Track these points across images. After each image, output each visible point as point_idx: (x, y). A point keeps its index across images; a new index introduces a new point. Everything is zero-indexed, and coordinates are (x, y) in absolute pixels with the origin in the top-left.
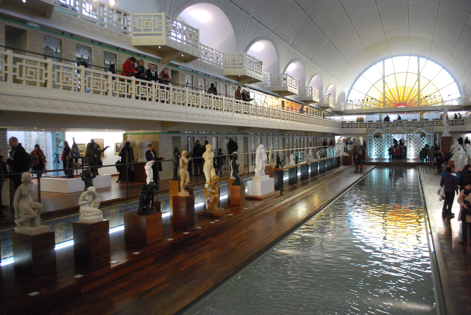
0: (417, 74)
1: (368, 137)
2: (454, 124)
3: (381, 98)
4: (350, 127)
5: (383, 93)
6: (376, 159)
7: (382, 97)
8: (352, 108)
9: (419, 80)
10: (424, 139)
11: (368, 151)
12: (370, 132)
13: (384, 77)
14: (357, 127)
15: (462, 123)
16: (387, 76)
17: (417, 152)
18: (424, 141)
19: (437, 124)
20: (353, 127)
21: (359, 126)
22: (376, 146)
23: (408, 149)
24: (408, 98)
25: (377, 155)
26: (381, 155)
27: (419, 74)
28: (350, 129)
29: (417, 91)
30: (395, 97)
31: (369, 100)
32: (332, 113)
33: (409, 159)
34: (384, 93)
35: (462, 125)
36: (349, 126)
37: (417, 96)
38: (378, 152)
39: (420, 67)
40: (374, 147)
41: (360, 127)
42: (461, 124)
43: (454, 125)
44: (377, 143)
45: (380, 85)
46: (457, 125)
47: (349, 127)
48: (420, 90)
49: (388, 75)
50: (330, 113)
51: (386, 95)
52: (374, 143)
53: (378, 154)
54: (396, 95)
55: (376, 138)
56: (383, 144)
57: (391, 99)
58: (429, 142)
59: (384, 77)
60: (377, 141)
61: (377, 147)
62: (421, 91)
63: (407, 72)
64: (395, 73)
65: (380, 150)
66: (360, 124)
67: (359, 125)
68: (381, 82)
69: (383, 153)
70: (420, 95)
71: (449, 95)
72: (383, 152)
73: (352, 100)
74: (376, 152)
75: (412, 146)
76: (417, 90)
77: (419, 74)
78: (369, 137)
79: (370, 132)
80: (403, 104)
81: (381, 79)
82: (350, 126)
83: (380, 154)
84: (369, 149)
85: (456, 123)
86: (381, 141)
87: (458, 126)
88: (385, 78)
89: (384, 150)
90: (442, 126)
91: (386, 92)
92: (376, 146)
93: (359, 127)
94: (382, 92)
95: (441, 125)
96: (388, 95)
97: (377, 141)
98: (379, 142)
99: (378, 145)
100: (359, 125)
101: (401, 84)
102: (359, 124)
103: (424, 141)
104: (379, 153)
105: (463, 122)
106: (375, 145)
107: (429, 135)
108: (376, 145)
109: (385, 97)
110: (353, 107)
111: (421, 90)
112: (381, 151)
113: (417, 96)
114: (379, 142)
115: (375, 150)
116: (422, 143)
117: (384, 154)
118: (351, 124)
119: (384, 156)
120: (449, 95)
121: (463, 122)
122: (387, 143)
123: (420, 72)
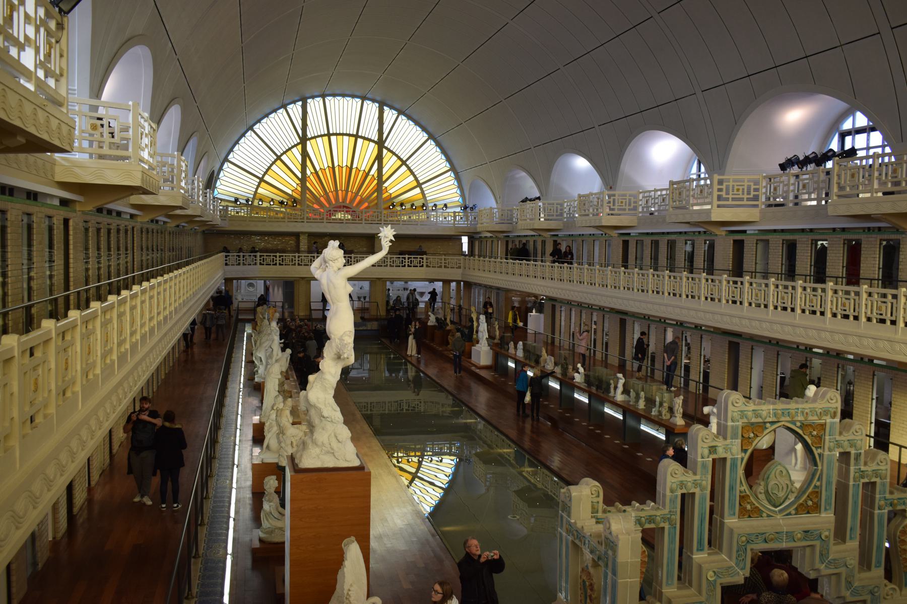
7: (299, 189)
9: (379, 158)
13: (304, 140)
16: (312, 138)
27: (380, 143)
29: (376, 182)
30: (328, 191)
37: (376, 194)
45: (294, 158)
49: (315, 137)
51: (308, 185)
54: (329, 186)
59: (304, 140)
63: (357, 136)
64: (329, 135)
68: (297, 152)
70: (382, 190)
77: (380, 143)
81: (298, 144)
88: (308, 142)
94: (300, 176)
111: (384, 178)
113: (376, 194)
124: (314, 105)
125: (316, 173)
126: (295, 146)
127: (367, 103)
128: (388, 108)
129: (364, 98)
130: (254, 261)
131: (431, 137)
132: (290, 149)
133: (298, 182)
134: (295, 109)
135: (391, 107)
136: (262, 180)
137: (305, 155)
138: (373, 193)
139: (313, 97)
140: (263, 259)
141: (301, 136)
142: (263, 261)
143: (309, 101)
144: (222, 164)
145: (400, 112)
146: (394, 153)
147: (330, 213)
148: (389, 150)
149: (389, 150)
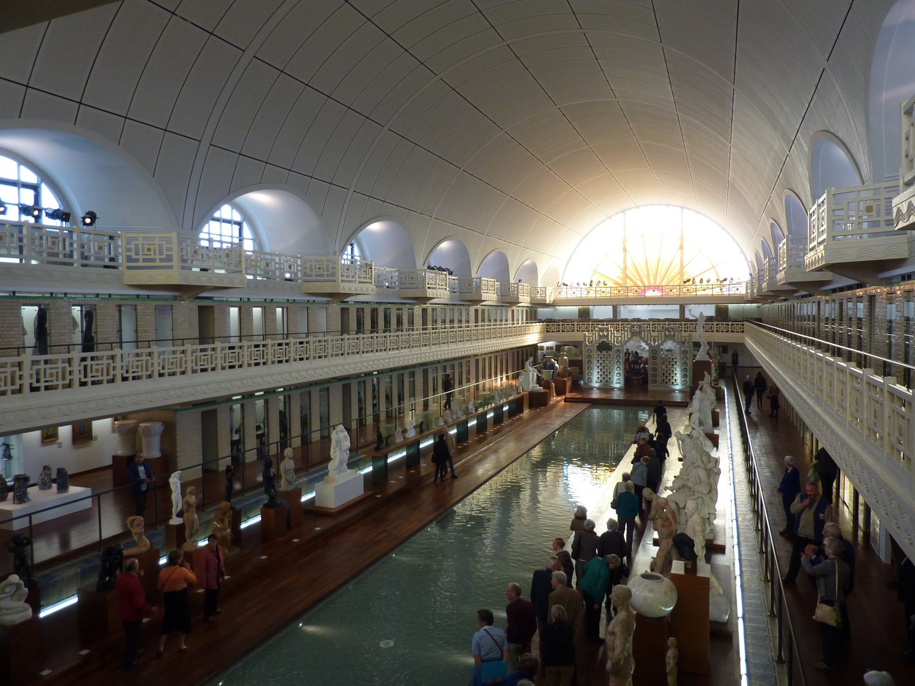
2: (730, 329)
3: (619, 277)
5: (622, 268)
7: (622, 276)
9: (681, 247)
14: (573, 331)
21: (576, 329)
24: (664, 278)
26: (607, 381)
29: (679, 266)
31: (594, 285)
34: (625, 268)
37: (679, 276)
38: (603, 376)
40: (596, 368)
41: (578, 331)
44: (600, 362)
47: (559, 331)
48: (684, 265)
51: (628, 272)
52: (596, 362)
55: (599, 353)
56: (610, 363)
57: (643, 273)
58: (686, 363)
61: (600, 368)
65: (606, 374)
66: (578, 325)
69: (610, 378)
70: (683, 273)
71: (725, 280)
73: (566, 283)
74: (599, 376)
76: (679, 264)
80: (655, 288)
82: (561, 329)
83: (606, 379)
93: (576, 330)
96: (631, 272)
97: (601, 358)
100: (576, 326)
102: (576, 325)
104: (604, 378)
108: (599, 365)
114: (603, 359)
116: (674, 363)
120: (725, 280)
138: (677, 275)
147: (644, 291)
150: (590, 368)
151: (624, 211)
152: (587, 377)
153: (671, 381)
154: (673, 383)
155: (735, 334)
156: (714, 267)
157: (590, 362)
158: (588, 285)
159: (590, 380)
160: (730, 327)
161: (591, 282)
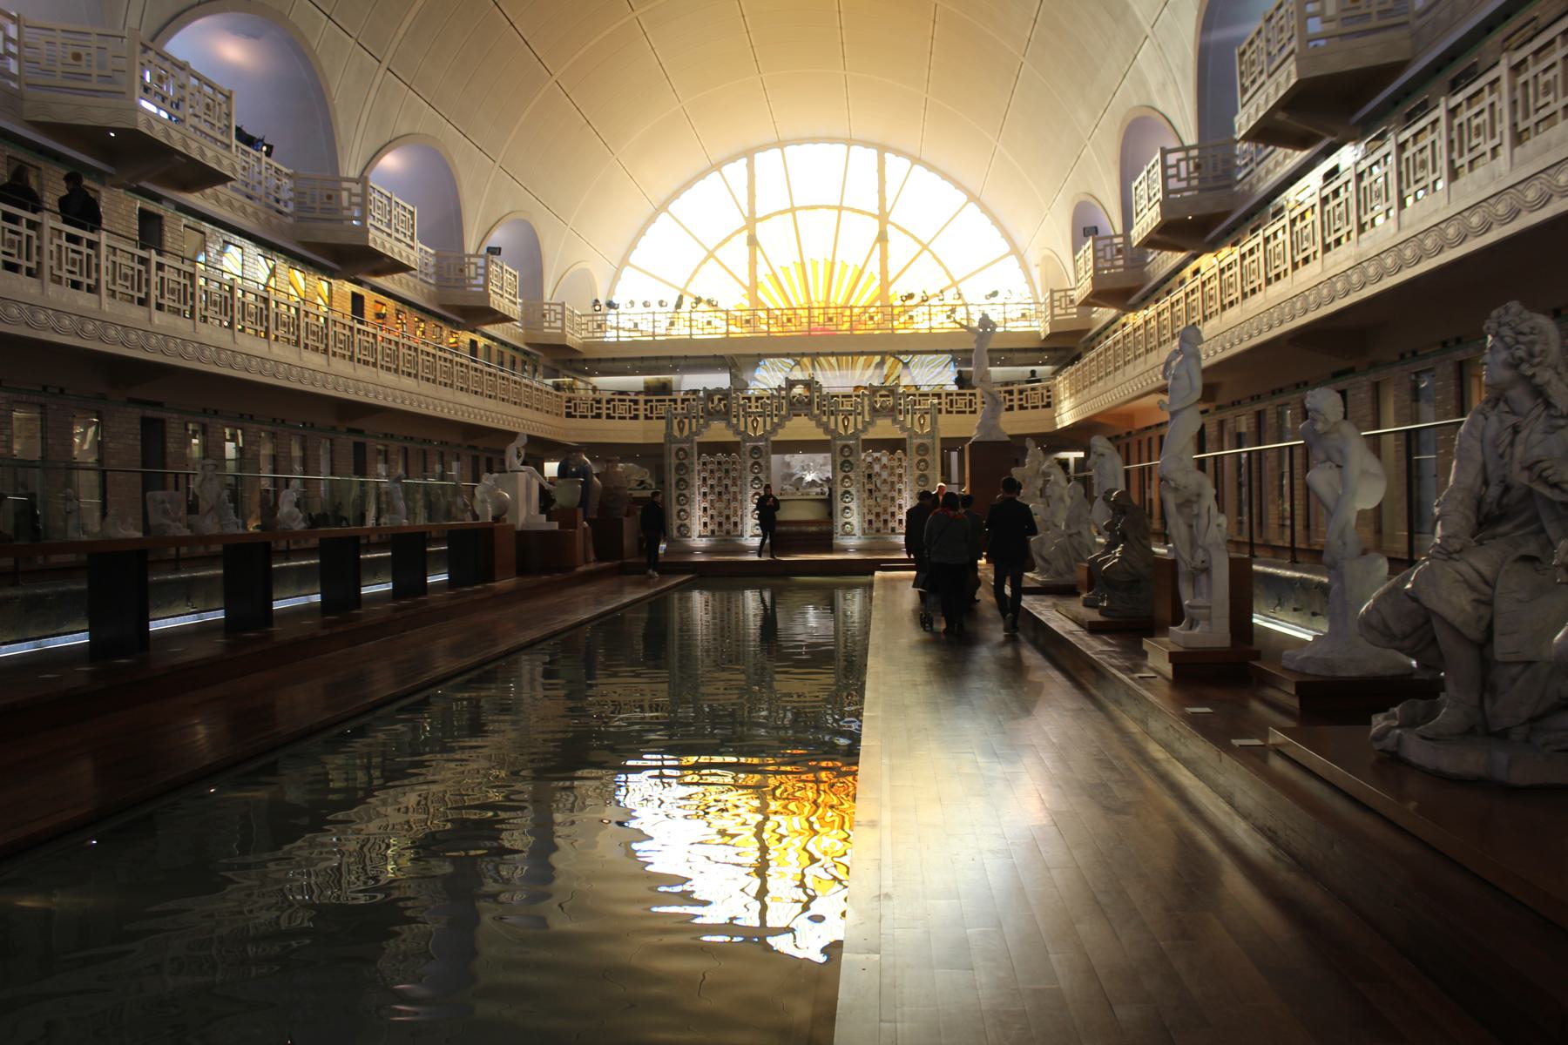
0: (874, 216)
1: (673, 452)
2: (1016, 403)
4: (604, 416)
5: (748, 284)
6: (705, 551)
7: (747, 304)
8: (618, 337)
9: (882, 238)
10: (900, 460)
11: (675, 517)
12: (681, 430)
14: (636, 417)
15: (1046, 400)
17: (872, 517)
18: (901, 471)
19: (951, 406)
20: (617, 415)
21: (642, 413)
22: (705, 494)
23: (840, 505)
25: (713, 532)
26: (728, 532)
27: (883, 217)
28: (603, 423)
29: (877, 282)
31: (686, 305)
32: (526, 353)
33: (844, 550)
35: (1044, 407)
36: (598, 408)
38: (717, 520)
39: (887, 187)
40: (698, 498)
41: (647, 417)
42: (1040, 404)
43: (1016, 407)
44: (709, 482)
45: (737, 252)
46: (1026, 408)
47: (598, 416)
48: (890, 279)
50: (516, 349)
51: (760, 294)
52: (698, 482)
53: (716, 528)
56: (735, 484)
59: (752, 221)
60: (712, 471)
61: (709, 498)
62: (890, 284)
66: (646, 402)
67: (641, 406)
69: (735, 524)
71: (995, 294)
72: (738, 519)
74: (707, 520)
75: (853, 490)
76: (878, 277)
78: (677, 454)
79: (681, 430)
82: (604, 412)
84: (675, 508)
85: (1024, 402)
86: (727, 471)
87: (1030, 411)
88: (758, 225)
89: (739, 513)
90: (971, 412)
91: (759, 280)
92: (705, 494)
93: (642, 417)
95: (968, 409)
97: (712, 471)
98: (717, 475)
99: (717, 490)
100: (641, 406)
101: (818, 250)
102: (642, 403)
103: (901, 471)
104: (720, 524)
105: (1049, 397)
106: (702, 490)
107: (922, 445)
109: (754, 299)
110: (622, 333)
112: (728, 517)
114: (717, 475)
115: (701, 513)
117: (740, 528)
118: (608, 402)
119: (742, 535)
120: (995, 294)
121: (1049, 397)
122: (751, 477)
123: (888, 210)
124: (767, 161)
125: (774, 274)
126: (739, 231)
127: (856, 150)
128: (893, 156)
129: (850, 142)
130: (633, 412)
131: (972, 197)
132: (727, 239)
133: (745, 292)
134: (736, 171)
135: (898, 153)
136: (684, 290)
137: (753, 241)
139: (764, 147)
140: (651, 407)
141: (747, 215)
142: (652, 413)
143: (758, 157)
144: (619, 271)
145: (916, 160)
146: (906, 232)
148: (898, 227)
149: (898, 227)
150: (683, 500)
151: (749, 154)
152: (676, 522)
153: (891, 525)
154: (893, 530)
155: (1030, 413)
156: (955, 284)
157: (683, 483)
158: (671, 307)
159: (684, 531)
160: (1016, 396)
161: (681, 298)
